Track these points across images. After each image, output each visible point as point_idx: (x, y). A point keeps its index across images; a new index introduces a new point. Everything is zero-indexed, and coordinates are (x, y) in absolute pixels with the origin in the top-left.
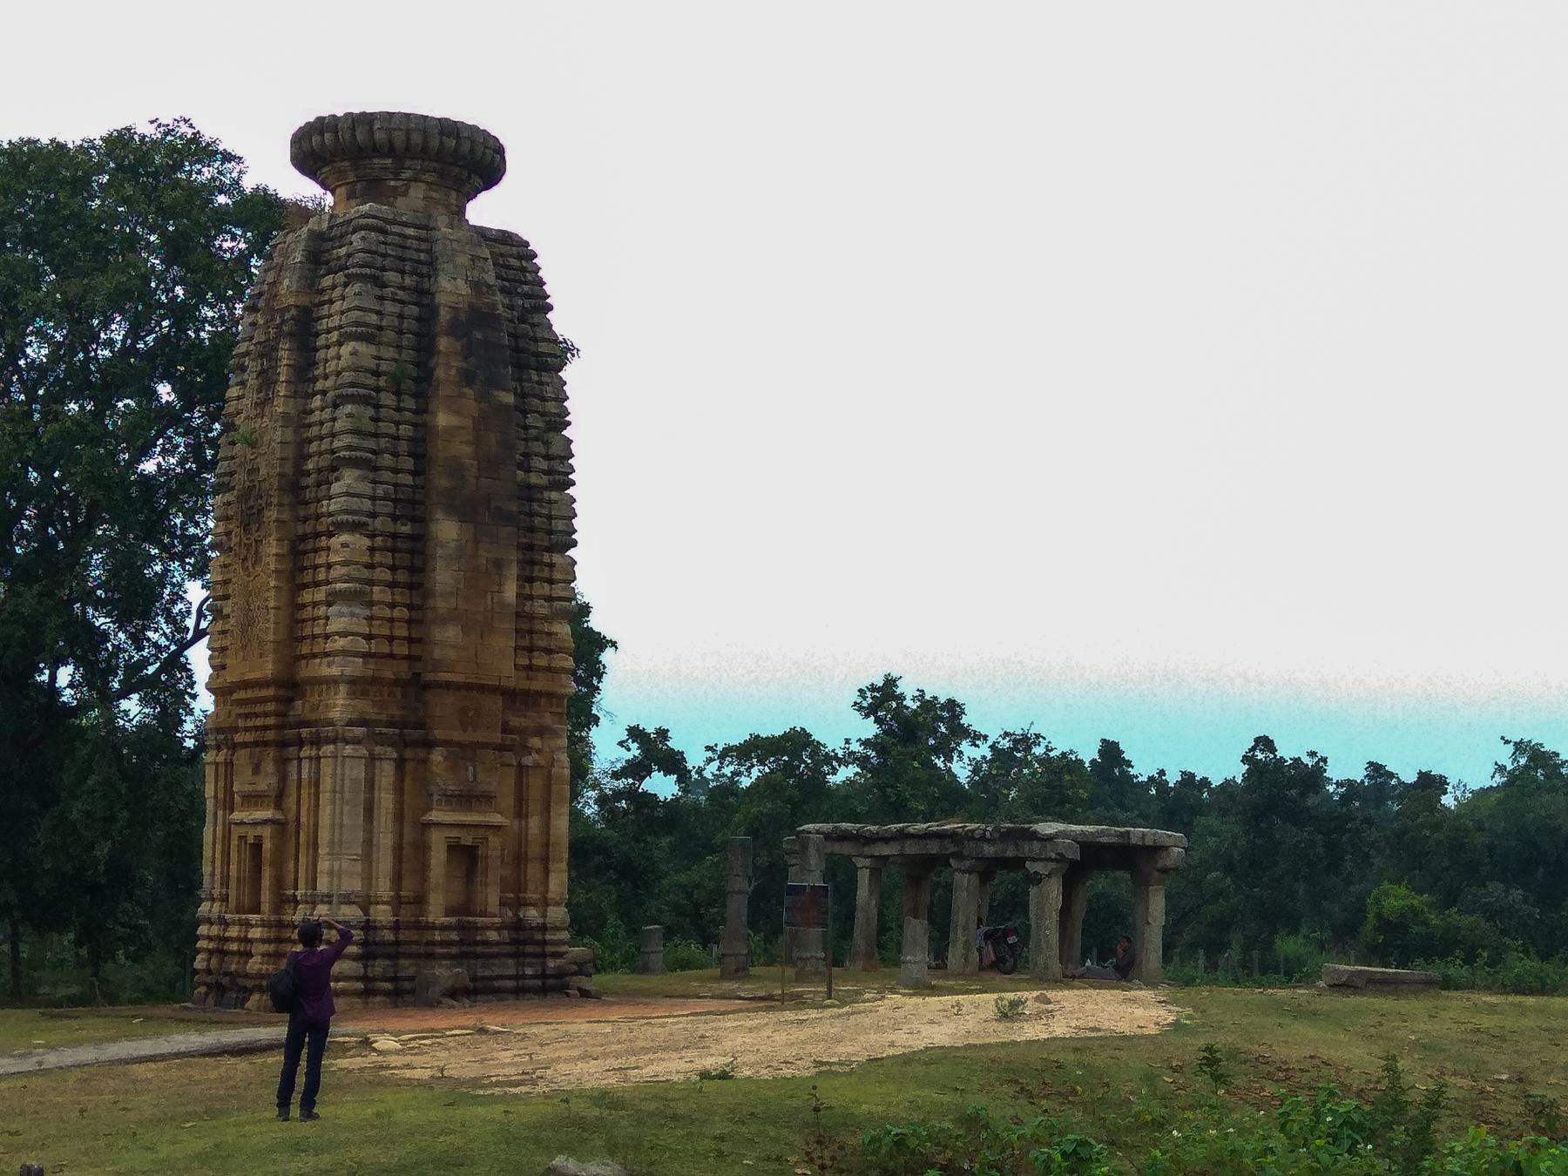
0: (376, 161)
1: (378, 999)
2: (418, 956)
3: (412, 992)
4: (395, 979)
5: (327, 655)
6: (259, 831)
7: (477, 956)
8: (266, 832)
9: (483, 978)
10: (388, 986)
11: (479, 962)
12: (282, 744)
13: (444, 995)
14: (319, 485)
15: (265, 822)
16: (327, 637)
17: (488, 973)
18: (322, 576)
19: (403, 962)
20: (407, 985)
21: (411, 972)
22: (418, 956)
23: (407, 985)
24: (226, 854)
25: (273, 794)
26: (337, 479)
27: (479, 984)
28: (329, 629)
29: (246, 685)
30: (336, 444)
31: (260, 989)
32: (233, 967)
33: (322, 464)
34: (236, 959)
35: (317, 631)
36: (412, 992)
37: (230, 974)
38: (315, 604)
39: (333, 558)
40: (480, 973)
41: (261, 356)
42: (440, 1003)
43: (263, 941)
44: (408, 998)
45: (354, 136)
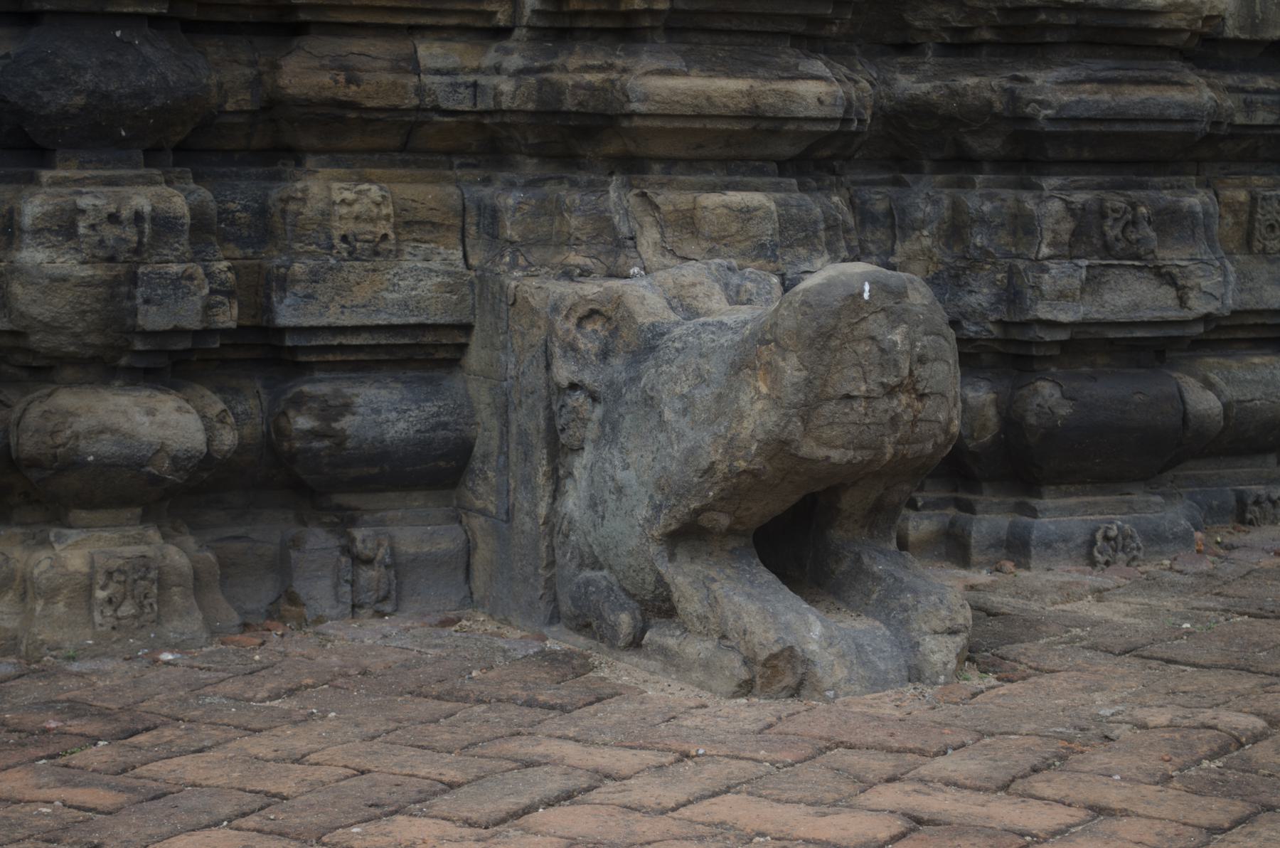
1: (75, 552)
2: (485, 141)
3: (439, 469)
4: (258, 353)
7: (1029, 150)
9: (1090, 345)
10: (167, 422)
11: (1053, 202)
13: (687, 535)
17: (1131, 298)
19: (336, 195)
20: (383, 411)
21: (416, 285)
22: (485, 141)
23: (383, 411)
27: (1048, 396)
36: (439, 469)
40: (1063, 296)
42: (660, 607)
44: (410, 529)
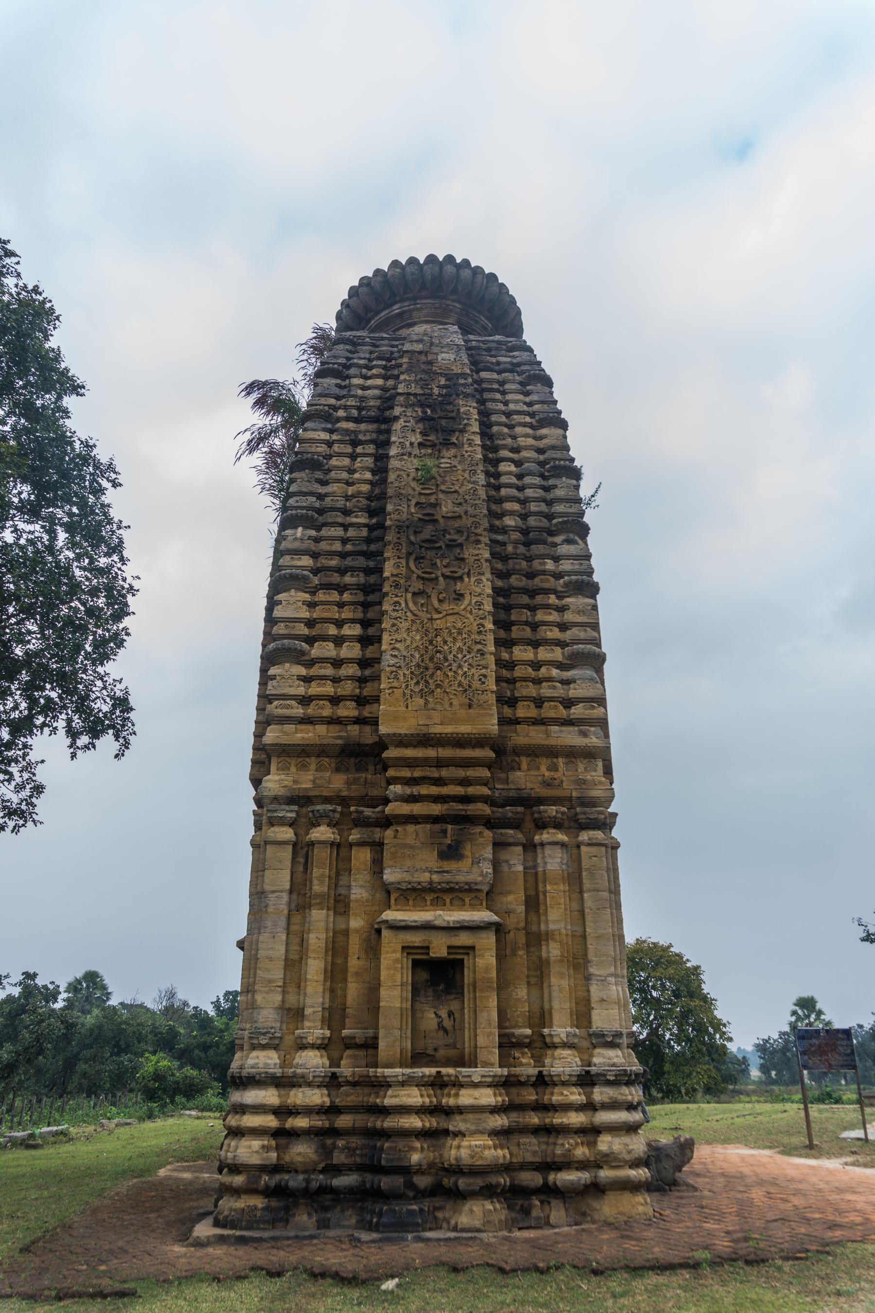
0: (483, 318)
5: (568, 722)
6: (464, 939)
8: (488, 940)
12: (490, 823)
14: (527, 544)
15: (485, 927)
16: (569, 703)
18: (554, 633)
24: (335, 974)
25: (486, 888)
26: (569, 542)
28: (574, 692)
29: (425, 740)
30: (559, 508)
31: (489, 1192)
32: (415, 1157)
33: (532, 521)
34: (418, 1145)
35: (546, 691)
37: (406, 1171)
38: (537, 665)
39: (569, 616)
41: (422, 405)
43: (495, 1110)
45: (487, 288)
